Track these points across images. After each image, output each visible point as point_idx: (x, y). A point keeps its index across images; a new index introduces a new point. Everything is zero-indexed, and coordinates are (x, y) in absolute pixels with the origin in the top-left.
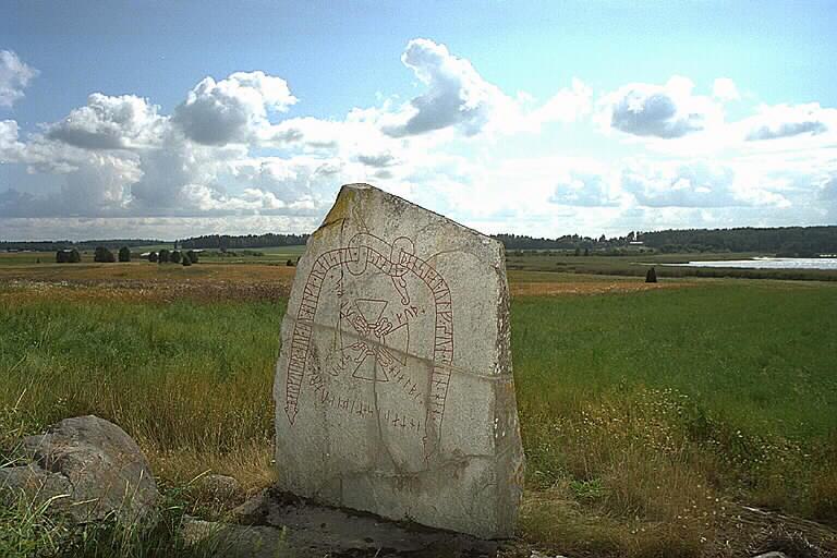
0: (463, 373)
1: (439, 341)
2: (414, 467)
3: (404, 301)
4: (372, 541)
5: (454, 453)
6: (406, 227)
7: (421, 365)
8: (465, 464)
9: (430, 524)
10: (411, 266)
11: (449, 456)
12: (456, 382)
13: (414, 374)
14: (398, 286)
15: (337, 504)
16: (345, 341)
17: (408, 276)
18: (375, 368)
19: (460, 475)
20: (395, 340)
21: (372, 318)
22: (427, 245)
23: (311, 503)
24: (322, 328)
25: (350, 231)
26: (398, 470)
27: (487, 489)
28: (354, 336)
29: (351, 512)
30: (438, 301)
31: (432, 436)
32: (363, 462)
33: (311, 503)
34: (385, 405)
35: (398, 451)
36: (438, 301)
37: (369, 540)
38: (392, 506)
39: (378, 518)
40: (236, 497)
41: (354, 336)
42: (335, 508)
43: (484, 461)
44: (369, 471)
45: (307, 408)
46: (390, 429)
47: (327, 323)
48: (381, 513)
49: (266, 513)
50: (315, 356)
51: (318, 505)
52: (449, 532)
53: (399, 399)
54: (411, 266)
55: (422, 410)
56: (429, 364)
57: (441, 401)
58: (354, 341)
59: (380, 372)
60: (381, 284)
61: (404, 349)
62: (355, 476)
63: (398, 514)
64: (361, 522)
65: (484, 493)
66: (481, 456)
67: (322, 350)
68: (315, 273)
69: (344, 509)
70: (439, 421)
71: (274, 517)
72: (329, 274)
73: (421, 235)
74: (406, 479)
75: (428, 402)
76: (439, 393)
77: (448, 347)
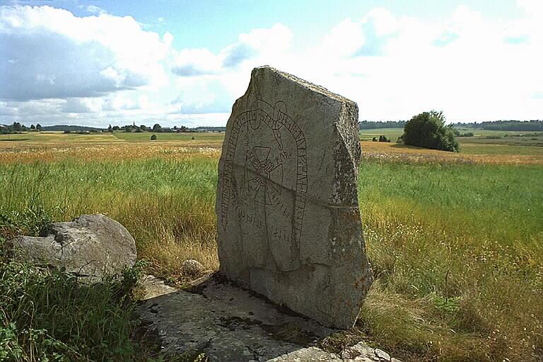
2: (285, 267)
4: (253, 314)
5: (307, 260)
7: (290, 194)
8: (313, 269)
11: (304, 262)
14: (276, 136)
20: (275, 176)
24: (237, 166)
27: (326, 289)
28: (254, 172)
31: (296, 247)
32: (259, 261)
37: (251, 314)
39: (267, 301)
40: (193, 273)
41: (254, 172)
44: (262, 268)
46: (273, 238)
49: (205, 287)
52: (307, 319)
56: (294, 194)
59: (267, 199)
61: (280, 183)
65: (324, 292)
71: (208, 291)
74: (282, 275)
75: (293, 221)
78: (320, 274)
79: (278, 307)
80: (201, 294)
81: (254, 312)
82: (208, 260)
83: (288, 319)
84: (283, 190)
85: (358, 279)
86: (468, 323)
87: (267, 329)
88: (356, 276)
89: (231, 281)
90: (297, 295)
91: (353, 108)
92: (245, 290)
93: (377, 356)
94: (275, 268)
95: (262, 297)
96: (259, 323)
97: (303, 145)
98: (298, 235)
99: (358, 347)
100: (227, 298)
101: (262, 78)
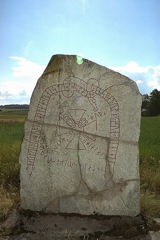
0: (125, 142)
1: (112, 128)
2: (99, 189)
3: (95, 109)
6: (94, 74)
7: (104, 140)
9: (107, 214)
10: (98, 92)
11: (117, 182)
12: (121, 147)
13: (101, 145)
15: (57, 212)
16: (62, 131)
17: (97, 98)
18: (78, 143)
21: (77, 119)
22: (105, 83)
24: (49, 125)
25: (64, 75)
26: (91, 191)
28: (66, 128)
29: (66, 215)
30: (112, 109)
31: (110, 173)
32: (71, 190)
33: (42, 213)
34: (84, 161)
35: (91, 183)
36: (112, 109)
38: (88, 208)
42: (56, 214)
43: (135, 182)
44: (74, 194)
45: (40, 167)
46: (87, 172)
47: (52, 122)
48: (82, 212)
50: (44, 139)
51: (46, 214)
53: (92, 159)
54: (98, 92)
55: (104, 162)
56: (108, 140)
57: (113, 156)
58: (67, 131)
60: (81, 101)
62: (66, 197)
63: (90, 212)
66: (133, 180)
68: (44, 97)
69: (61, 214)
70: (113, 166)
72: (52, 97)
73: (102, 77)
74: (94, 194)
75: (107, 158)
76: (113, 153)
77: (117, 130)
79: (91, 217)
81: (86, 228)
84: (97, 139)
89: (37, 212)
94: (88, 192)
97: (117, 108)
101: (58, 63)
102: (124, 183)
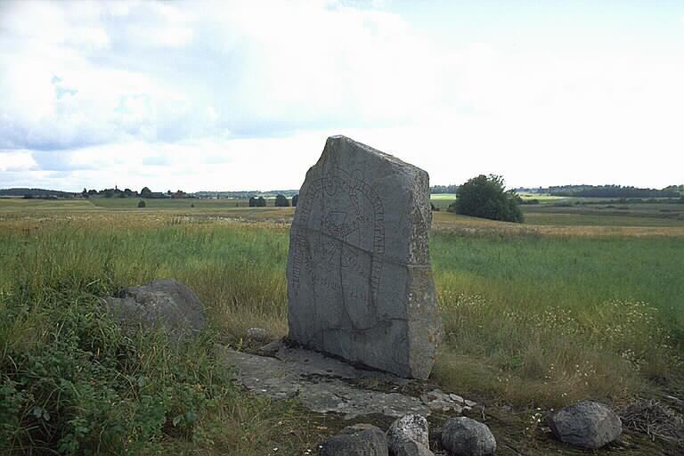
2: (362, 326)
5: (384, 316)
7: (367, 256)
8: (390, 324)
11: (382, 319)
19: (388, 331)
23: (306, 348)
31: (372, 304)
39: (343, 360)
40: (264, 341)
44: (337, 329)
50: (308, 249)
52: (385, 372)
55: (367, 287)
59: (344, 262)
64: (331, 360)
66: (400, 319)
67: (312, 245)
71: (280, 354)
74: (358, 333)
78: (397, 327)
80: (274, 357)
82: (279, 327)
83: (365, 373)
85: (432, 333)
86: (534, 372)
87: (348, 382)
88: (430, 330)
90: (374, 351)
91: (424, 176)
92: (318, 352)
93: (451, 399)
95: (335, 357)
96: (339, 377)
98: (375, 294)
99: (435, 393)
100: (303, 360)
102: (387, 323)
